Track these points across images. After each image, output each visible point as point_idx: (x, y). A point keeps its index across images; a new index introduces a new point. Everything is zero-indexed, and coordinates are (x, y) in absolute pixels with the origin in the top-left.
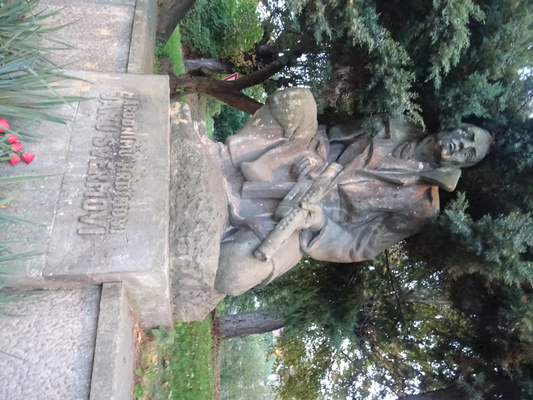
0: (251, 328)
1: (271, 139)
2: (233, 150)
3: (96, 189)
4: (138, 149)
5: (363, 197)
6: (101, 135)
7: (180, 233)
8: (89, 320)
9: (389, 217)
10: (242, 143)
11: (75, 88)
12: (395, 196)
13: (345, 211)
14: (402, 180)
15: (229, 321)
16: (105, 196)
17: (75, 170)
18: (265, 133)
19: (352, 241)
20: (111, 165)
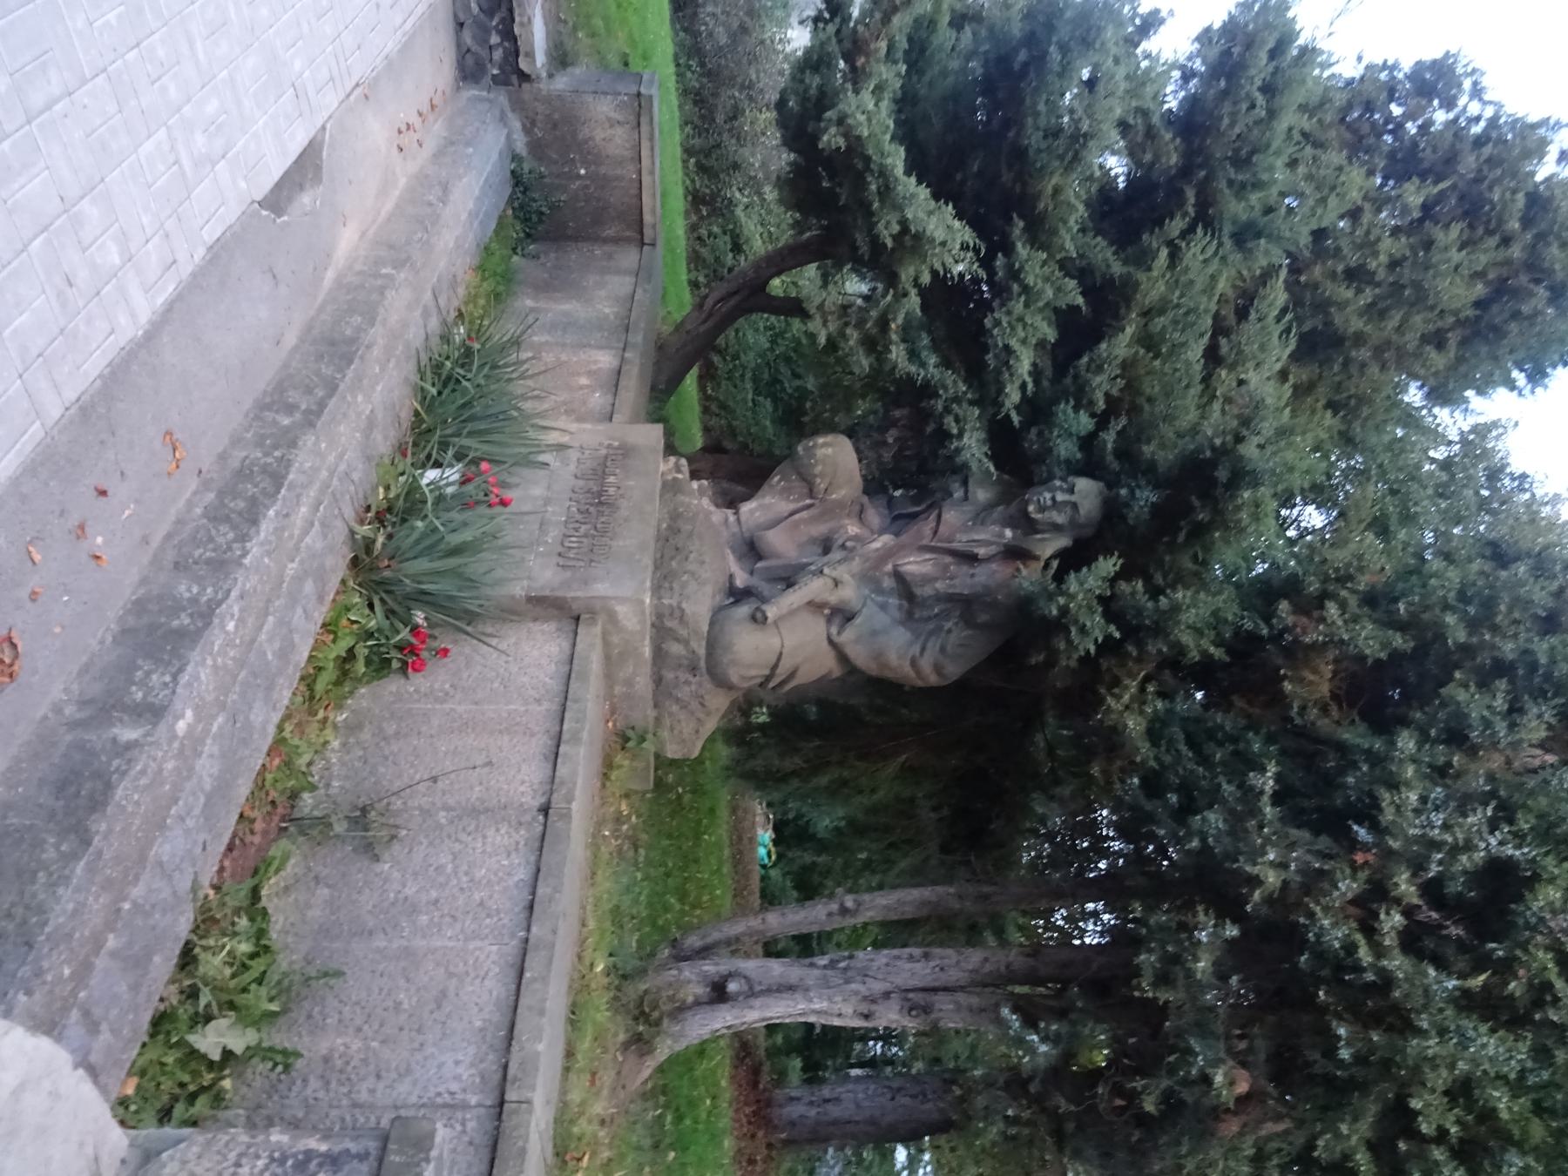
0: (857, 1122)
1: (794, 501)
2: (743, 518)
3: (576, 530)
4: (622, 496)
5: (927, 580)
6: (581, 483)
7: (664, 578)
8: (566, 645)
9: (965, 605)
10: (756, 509)
11: (553, 438)
12: (973, 576)
13: (905, 604)
14: (976, 551)
15: (798, 1099)
16: (585, 536)
17: (553, 513)
18: (786, 492)
19: (911, 644)
20: (592, 509)
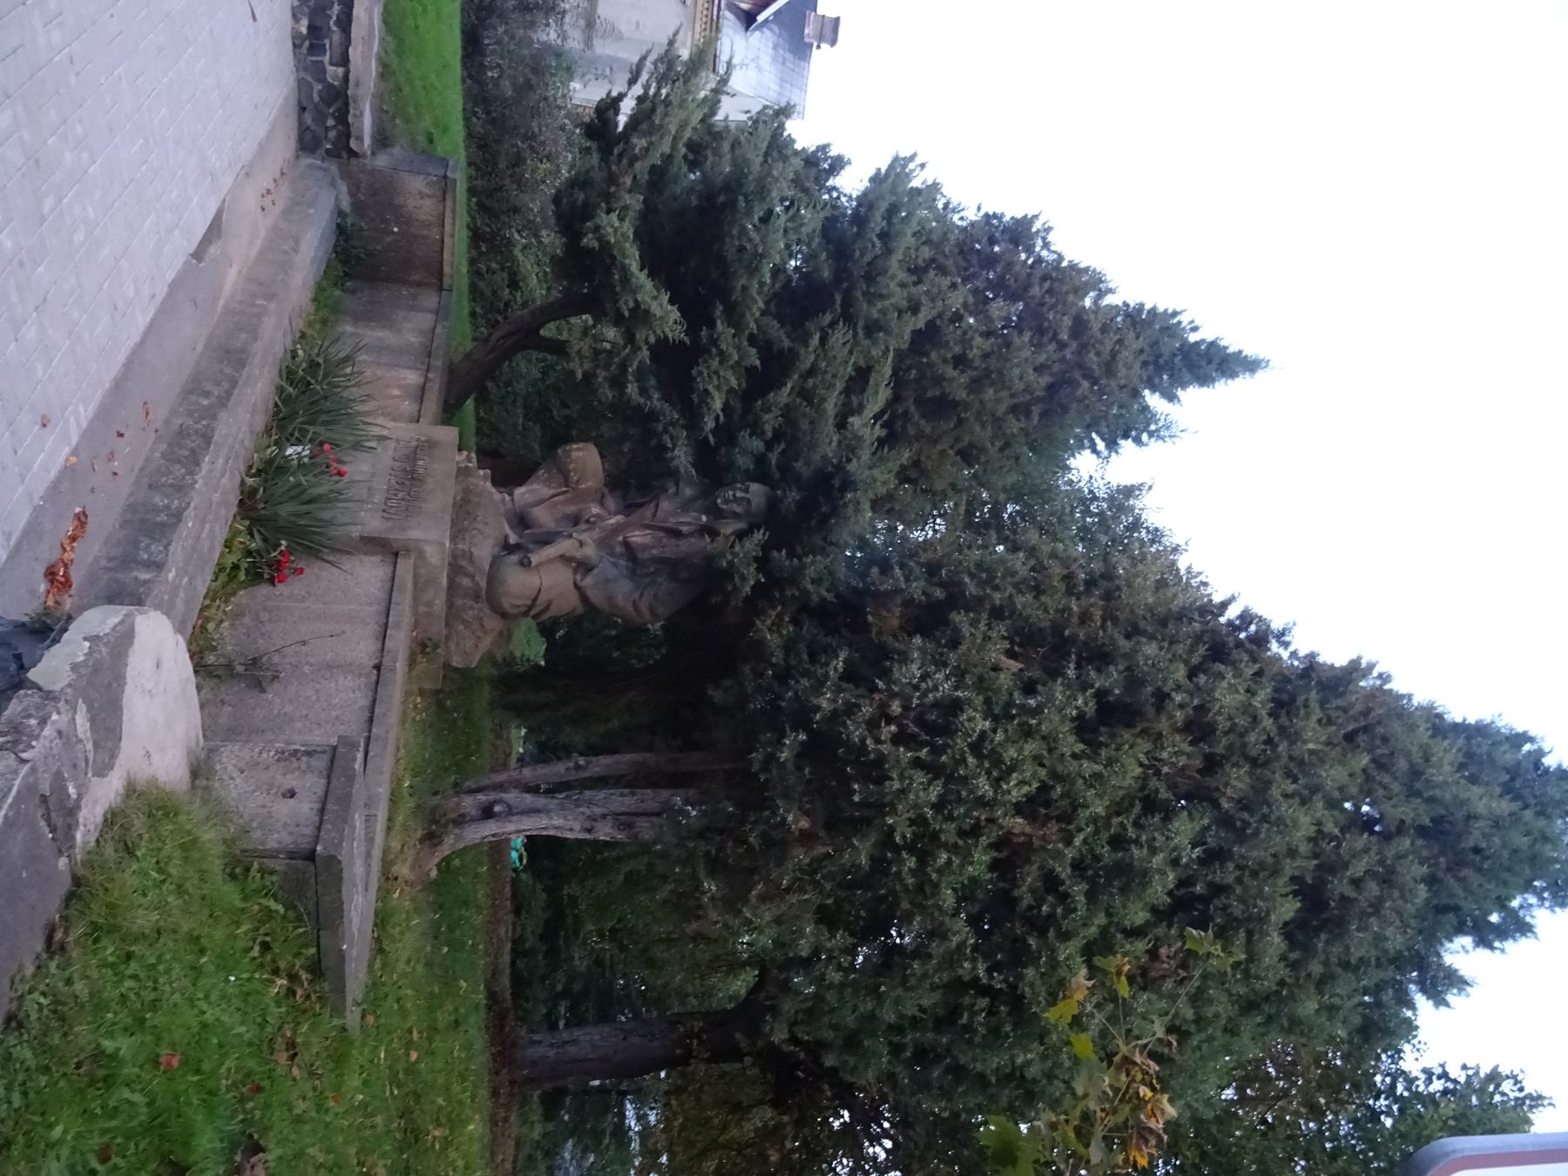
5: (645, 547)
7: (457, 532)
8: (389, 571)
9: (672, 566)
11: (376, 431)
15: (540, 1042)
18: (547, 482)
